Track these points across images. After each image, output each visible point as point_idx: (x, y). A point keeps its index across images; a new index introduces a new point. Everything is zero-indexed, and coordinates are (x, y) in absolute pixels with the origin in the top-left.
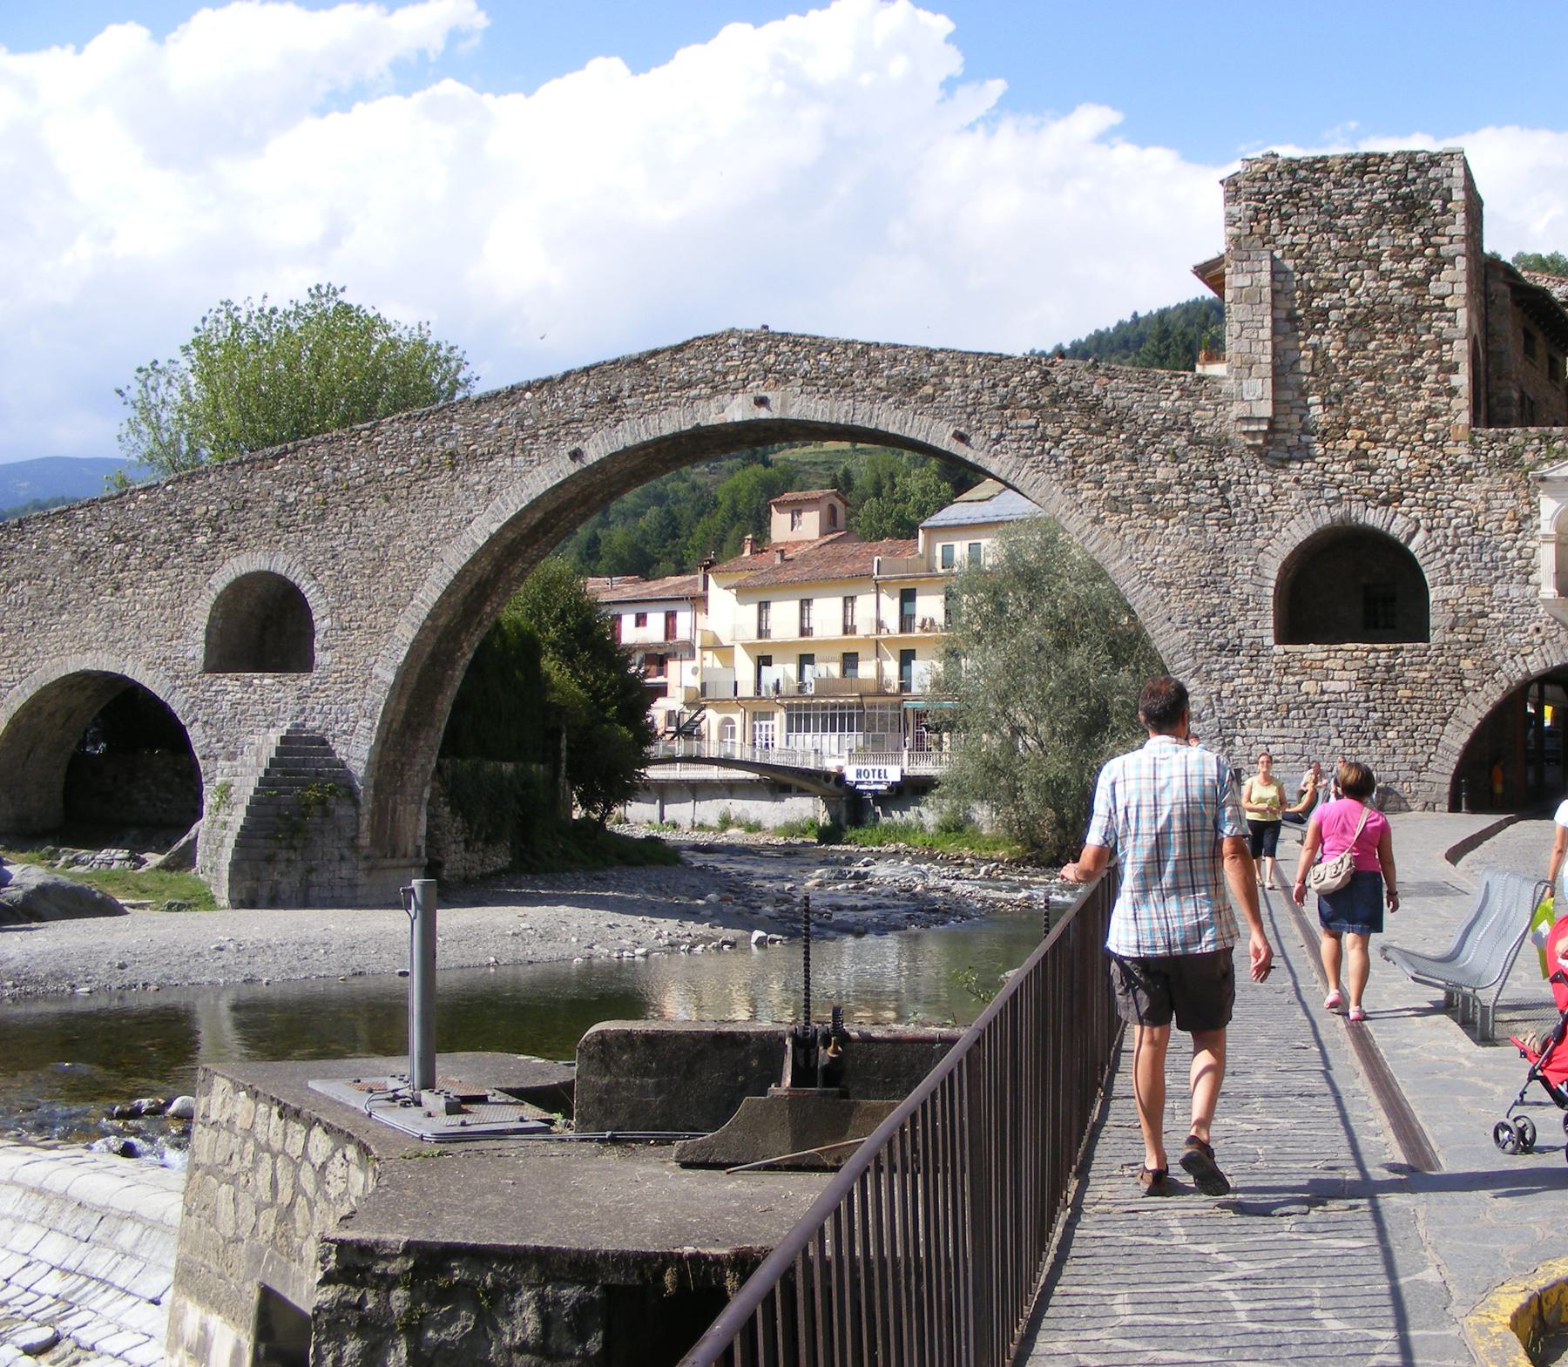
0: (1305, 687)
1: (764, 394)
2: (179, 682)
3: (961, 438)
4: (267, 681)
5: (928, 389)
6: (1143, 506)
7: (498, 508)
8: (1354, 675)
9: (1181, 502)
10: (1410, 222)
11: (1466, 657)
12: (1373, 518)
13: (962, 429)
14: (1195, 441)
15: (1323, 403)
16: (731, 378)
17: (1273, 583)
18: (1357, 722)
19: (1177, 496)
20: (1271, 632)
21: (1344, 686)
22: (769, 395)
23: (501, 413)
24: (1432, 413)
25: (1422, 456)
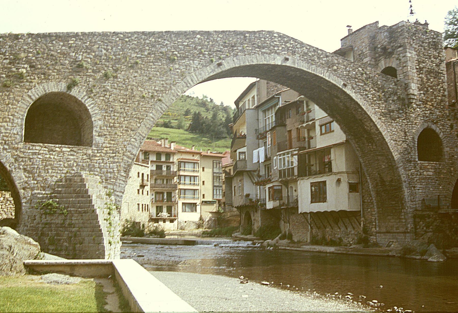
0: (425, 173)
1: (287, 57)
2: (6, 147)
3: (345, 85)
4: (64, 149)
5: (335, 67)
6: (389, 116)
7: (188, 81)
8: (433, 170)
9: (397, 116)
10: (436, 49)
11: (452, 167)
12: (433, 127)
13: (345, 83)
14: (399, 98)
15: (424, 94)
16: (276, 48)
17: (416, 143)
18: (434, 184)
19: (395, 114)
20: (417, 157)
21: (431, 173)
22: (290, 58)
23: (187, 41)
24: (442, 101)
25: (440, 112)
